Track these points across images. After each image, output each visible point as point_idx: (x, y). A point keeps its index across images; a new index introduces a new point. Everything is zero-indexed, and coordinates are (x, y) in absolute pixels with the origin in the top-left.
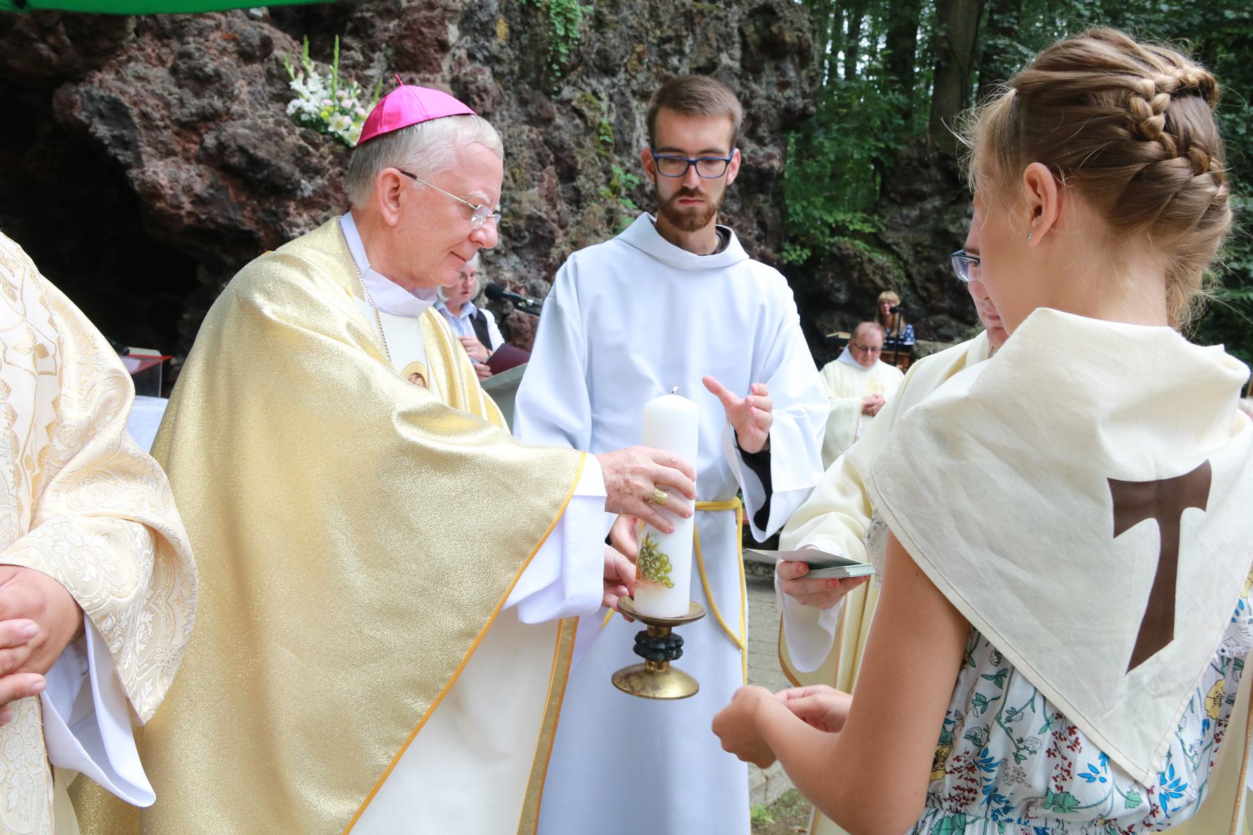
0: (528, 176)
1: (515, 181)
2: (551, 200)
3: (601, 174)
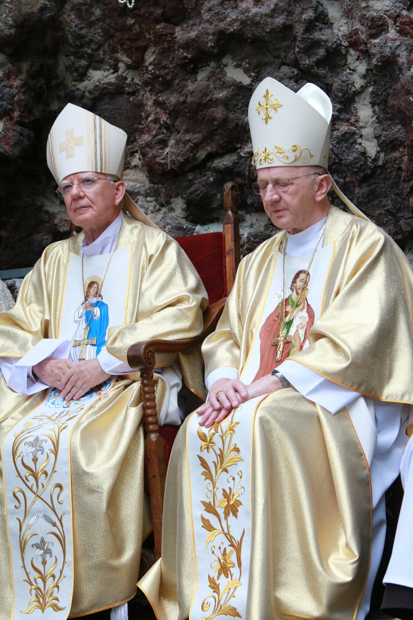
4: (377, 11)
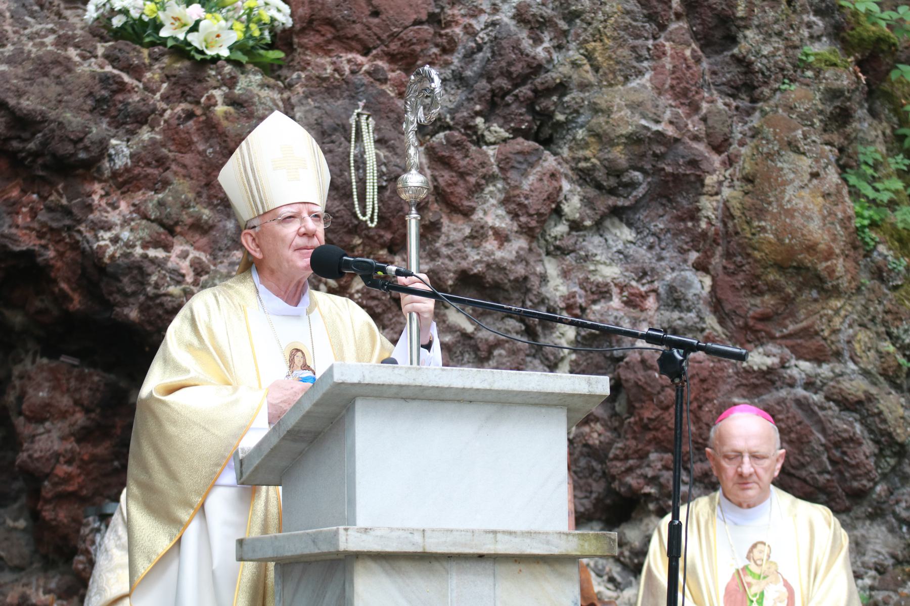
0: (625, 52)
1: (596, 69)
2: (685, 95)
3: (813, 18)
4: (604, 277)
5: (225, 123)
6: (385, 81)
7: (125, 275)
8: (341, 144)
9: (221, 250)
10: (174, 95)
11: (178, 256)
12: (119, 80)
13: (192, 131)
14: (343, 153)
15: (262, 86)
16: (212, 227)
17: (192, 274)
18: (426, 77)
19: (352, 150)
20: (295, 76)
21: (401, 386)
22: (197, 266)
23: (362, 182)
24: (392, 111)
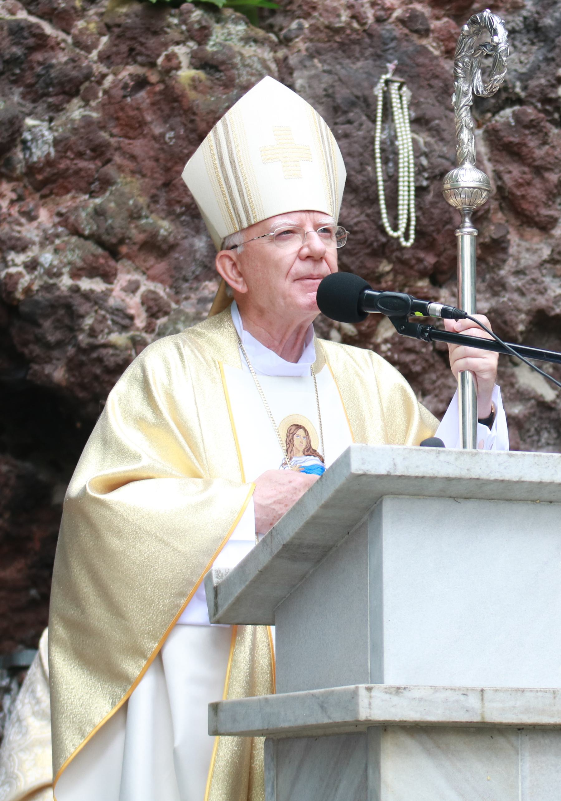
5: (192, 95)
6: (425, 33)
7: (46, 316)
8: (361, 125)
9: (186, 280)
10: (118, 53)
11: (124, 290)
12: (38, 31)
13: (144, 106)
14: (365, 138)
15: (247, 40)
16: (173, 247)
17: (144, 315)
18: (485, 27)
19: (378, 134)
20: (294, 25)
21: (448, 479)
22: (151, 303)
23: (392, 181)
24: (437, 77)
